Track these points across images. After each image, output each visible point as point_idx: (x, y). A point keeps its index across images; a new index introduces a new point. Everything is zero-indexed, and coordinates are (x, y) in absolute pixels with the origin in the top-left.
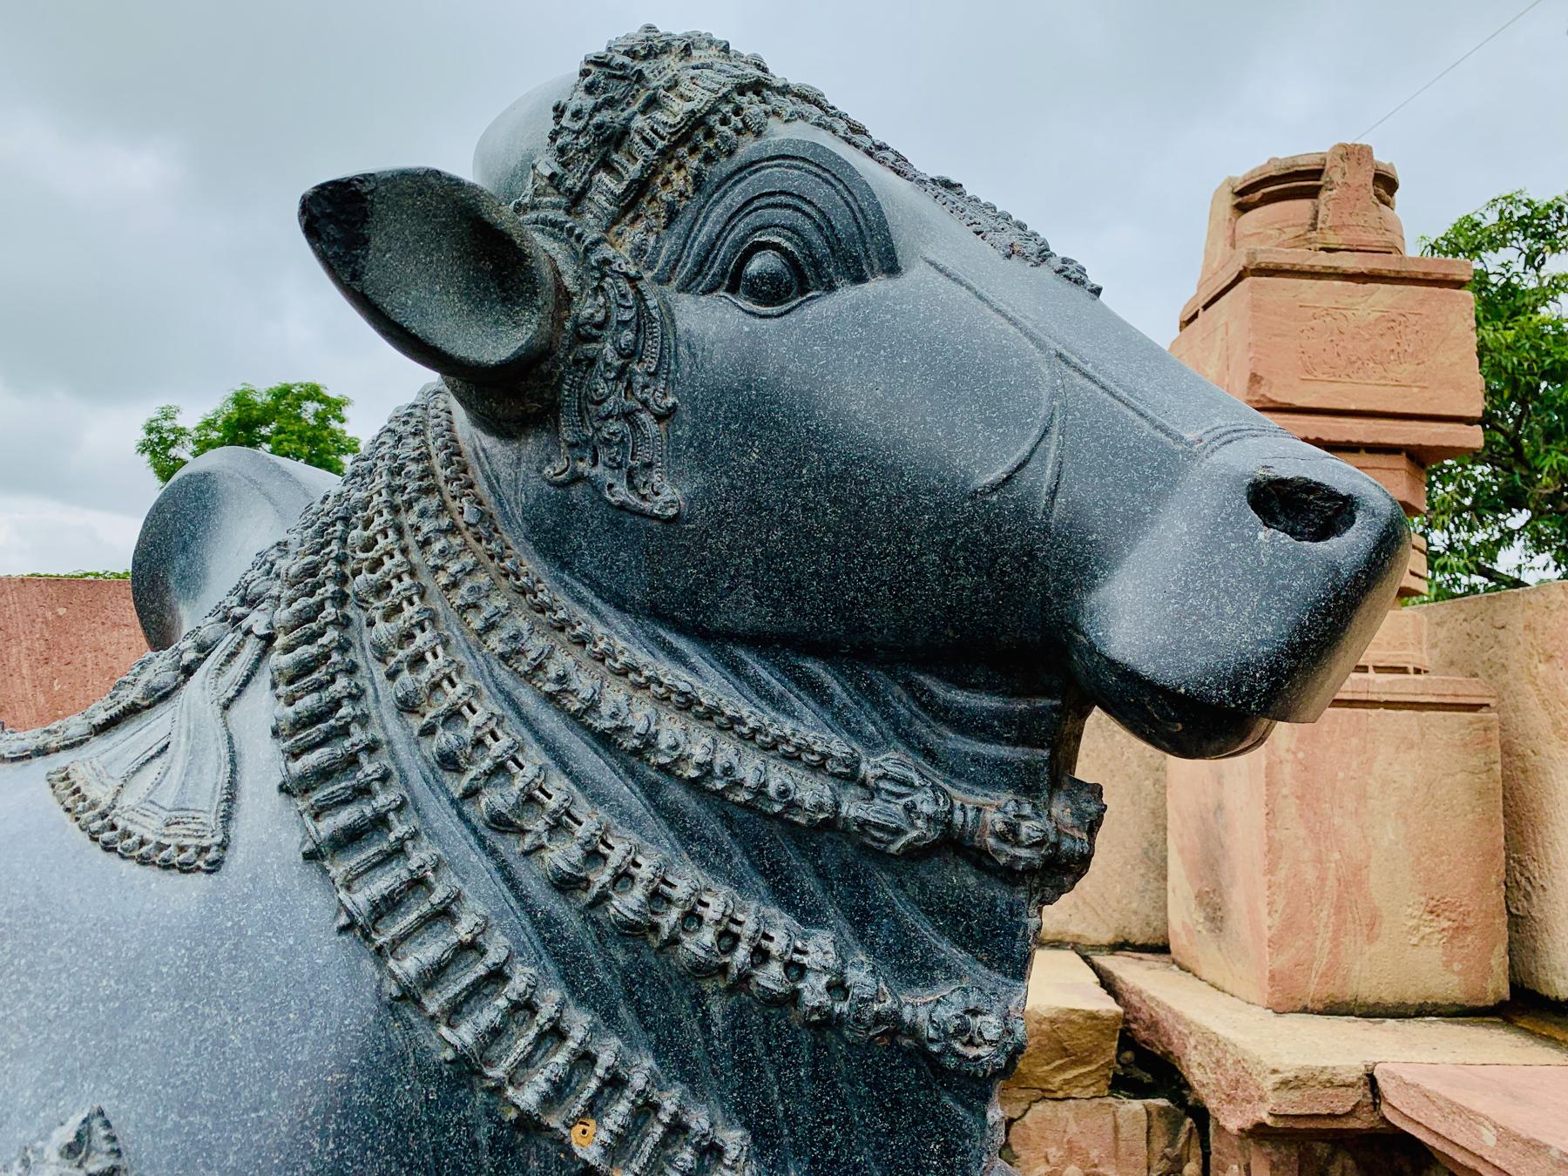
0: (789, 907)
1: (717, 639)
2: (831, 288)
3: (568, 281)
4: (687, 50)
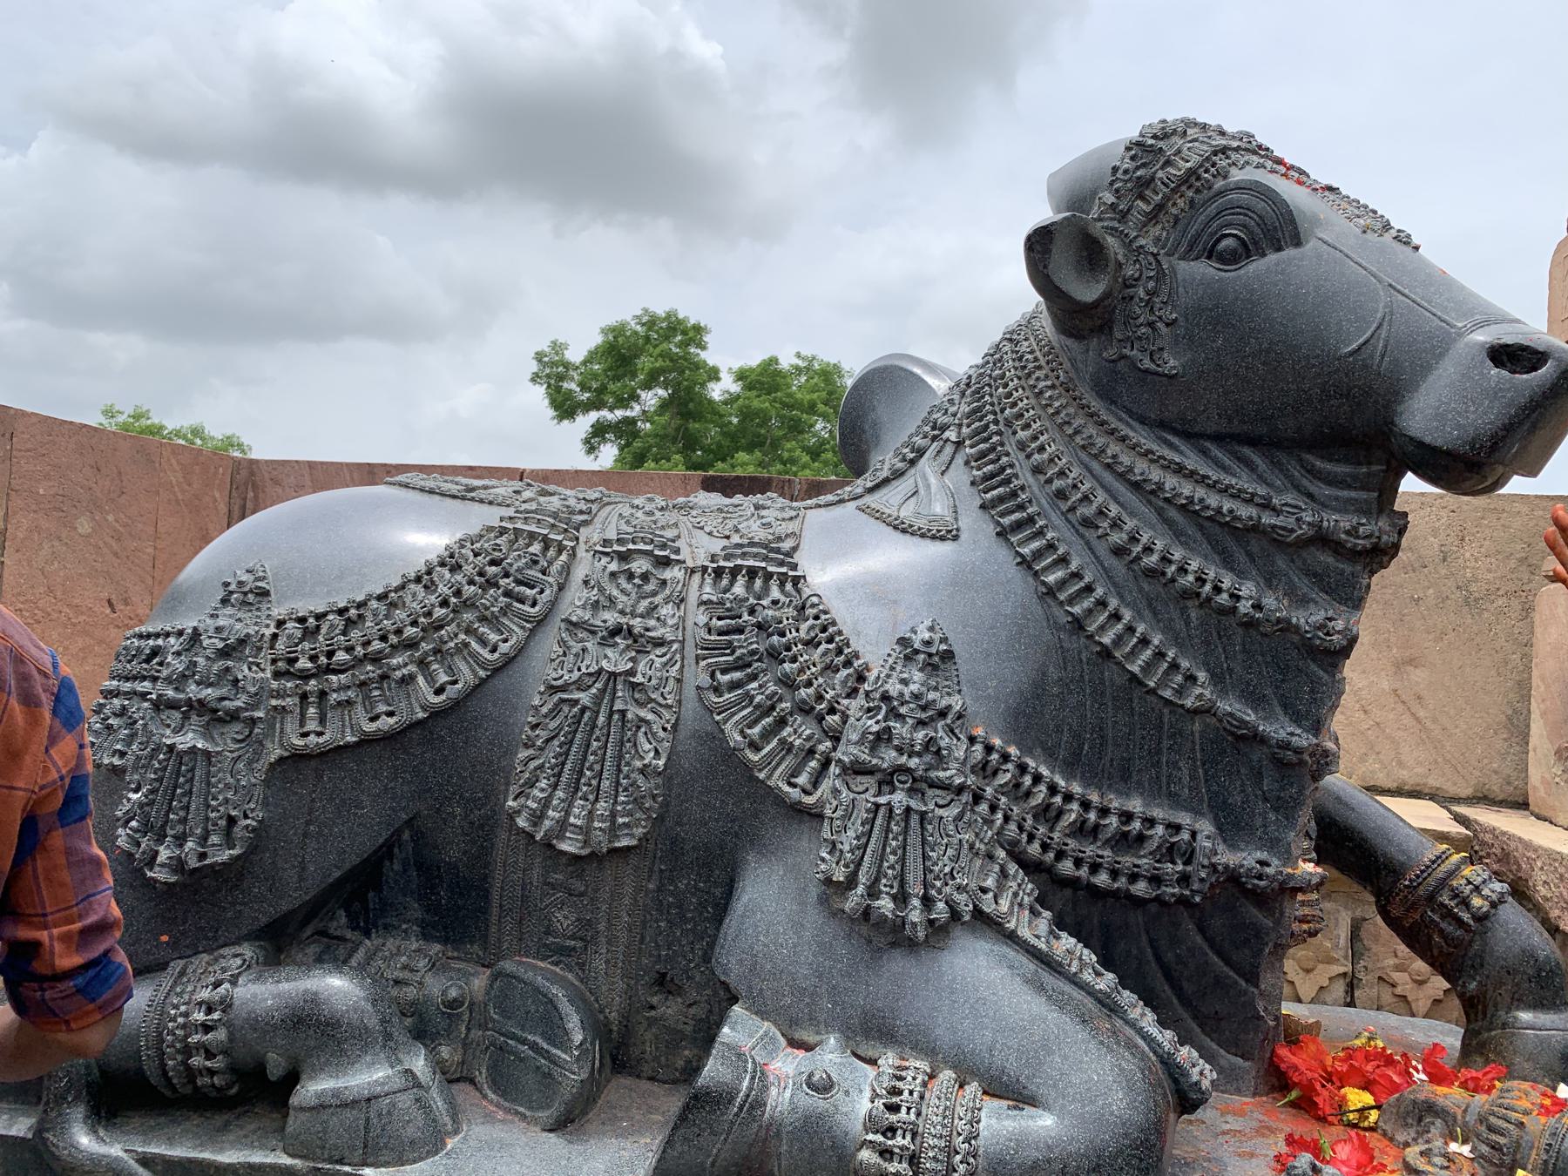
0: (1232, 570)
2: (1264, 255)
3: (1120, 257)
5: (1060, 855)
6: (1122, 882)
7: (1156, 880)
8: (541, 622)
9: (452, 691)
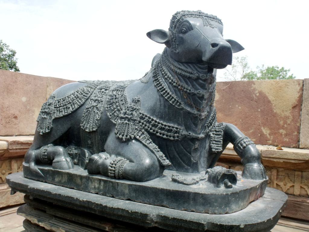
1: (182, 63)
4: (179, 13)
5: (157, 132)
7: (174, 137)
8: (87, 99)
9: (74, 109)
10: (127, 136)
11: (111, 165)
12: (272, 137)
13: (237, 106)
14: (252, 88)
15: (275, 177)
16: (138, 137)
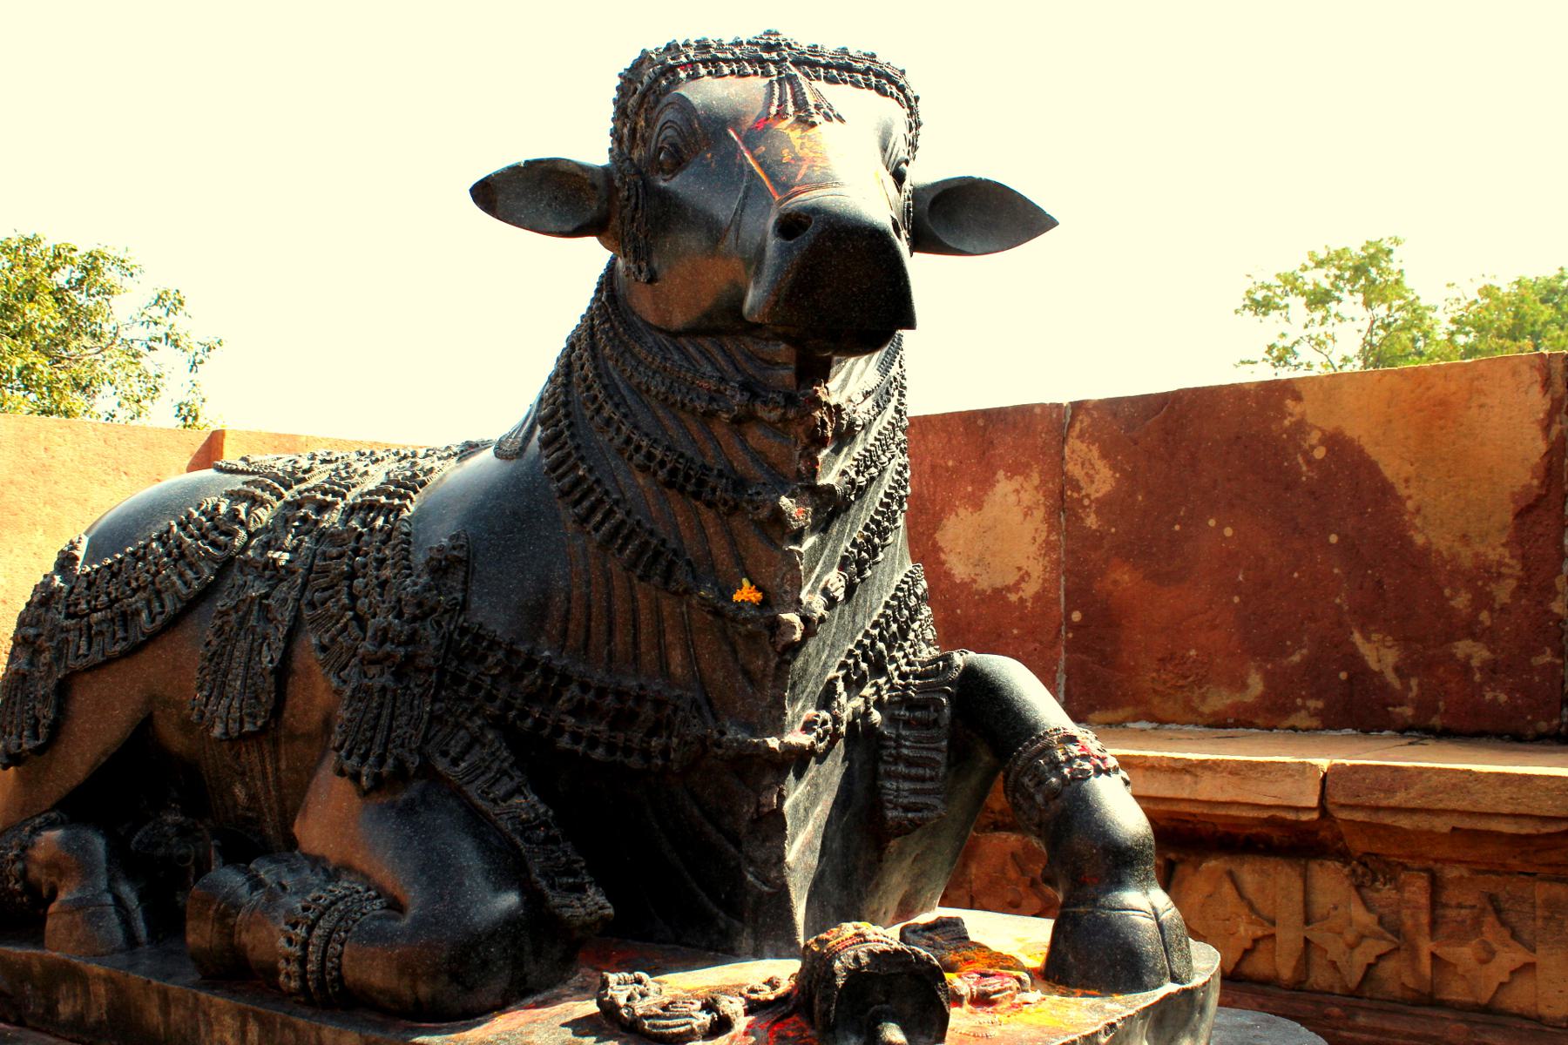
6: (619, 756)
10: (381, 760)
11: (288, 928)
12: (1414, 682)
13: (1212, 523)
14: (1287, 422)
15: (1424, 918)
16: (441, 765)
